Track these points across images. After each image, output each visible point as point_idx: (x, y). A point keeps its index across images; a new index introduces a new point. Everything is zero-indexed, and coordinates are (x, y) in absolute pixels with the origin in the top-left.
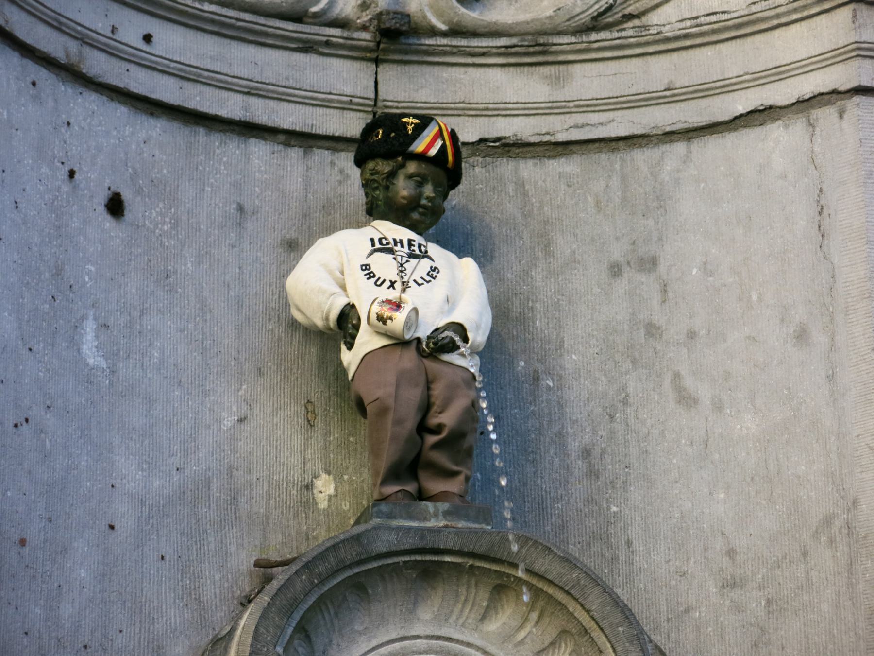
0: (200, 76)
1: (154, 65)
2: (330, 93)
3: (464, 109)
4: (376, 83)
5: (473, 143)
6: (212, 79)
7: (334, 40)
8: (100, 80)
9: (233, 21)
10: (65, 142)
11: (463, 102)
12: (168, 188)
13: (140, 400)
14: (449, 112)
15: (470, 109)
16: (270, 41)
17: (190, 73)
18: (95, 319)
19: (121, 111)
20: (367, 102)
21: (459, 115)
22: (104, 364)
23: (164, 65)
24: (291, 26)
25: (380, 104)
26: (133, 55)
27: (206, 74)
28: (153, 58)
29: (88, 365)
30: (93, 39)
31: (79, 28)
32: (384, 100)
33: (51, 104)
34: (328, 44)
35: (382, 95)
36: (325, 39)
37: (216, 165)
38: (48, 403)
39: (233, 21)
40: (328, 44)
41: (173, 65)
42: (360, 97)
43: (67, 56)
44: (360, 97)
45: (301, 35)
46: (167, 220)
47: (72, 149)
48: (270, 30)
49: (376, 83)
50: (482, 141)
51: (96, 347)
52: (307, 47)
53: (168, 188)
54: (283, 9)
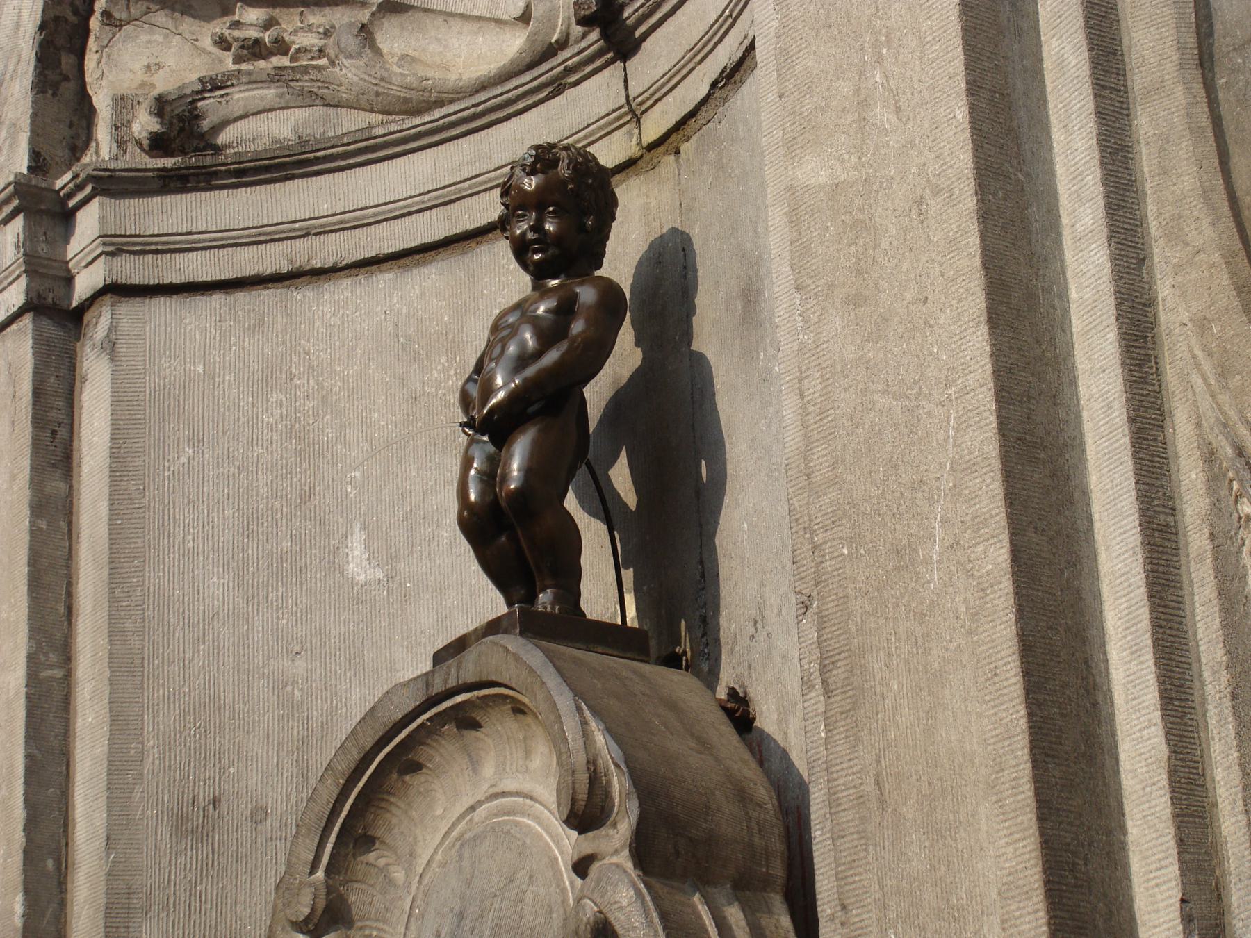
0: (461, 190)
1: (406, 210)
2: (589, 126)
3: (691, 59)
4: (626, 81)
5: (709, 94)
6: (475, 185)
7: (569, 63)
8: (344, 263)
9: (472, 110)
10: (308, 354)
11: (688, 52)
12: (451, 336)
13: (429, 596)
14: (685, 71)
15: (695, 55)
16: (521, 105)
17: (449, 194)
18: (364, 527)
19: (385, 279)
20: (622, 111)
21: (693, 69)
22: (379, 574)
23: (417, 204)
24: (527, 77)
25: (634, 105)
26: (379, 214)
27: (466, 184)
28: (402, 203)
29: (353, 583)
30: (322, 226)
31: (297, 225)
32: (635, 98)
33: (281, 320)
34: (569, 71)
35: (632, 94)
36: (561, 68)
37: (503, 279)
38: (297, 649)
39: (472, 110)
40: (569, 71)
41: (428, 196)
42: (614, 111)
43: (290, 261)
44: (614, 111)
45: (540, 80)
46: (452, 372)
47: (318, 357)
48: (510, 95)
49: (626, 81)
50: (714, 85)
51: (369, 559)
52: (557, 87)
53: (451, 336)
54: (528, 60)
